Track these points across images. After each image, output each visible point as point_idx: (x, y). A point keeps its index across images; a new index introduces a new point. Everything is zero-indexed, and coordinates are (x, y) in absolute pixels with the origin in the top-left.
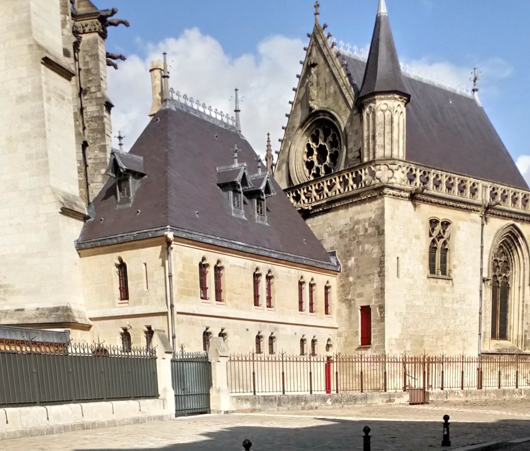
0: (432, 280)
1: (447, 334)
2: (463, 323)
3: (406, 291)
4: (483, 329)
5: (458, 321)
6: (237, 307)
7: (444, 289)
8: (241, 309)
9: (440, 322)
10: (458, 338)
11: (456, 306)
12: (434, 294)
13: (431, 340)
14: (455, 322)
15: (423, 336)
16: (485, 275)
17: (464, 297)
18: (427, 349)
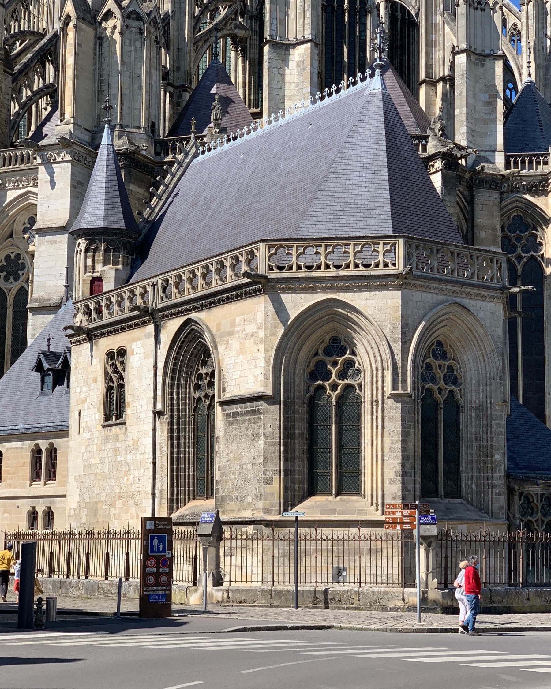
0: (107, 429)
1: (120, 497)
2: (136, 479)
3: (83, 449)
4: (158, 486)
5: (131, 478)
6: (10, 486)
7: (117, 437)
8: (14, 487)
9: (113, 482)
10: (131, 502)
11: (129, 457)
12: (109, 446)
13: (104, 507)
14: (128, 480)
15: (97, 503)
16: (159, 407)
17: (137, 444)
18: (100, 520)
